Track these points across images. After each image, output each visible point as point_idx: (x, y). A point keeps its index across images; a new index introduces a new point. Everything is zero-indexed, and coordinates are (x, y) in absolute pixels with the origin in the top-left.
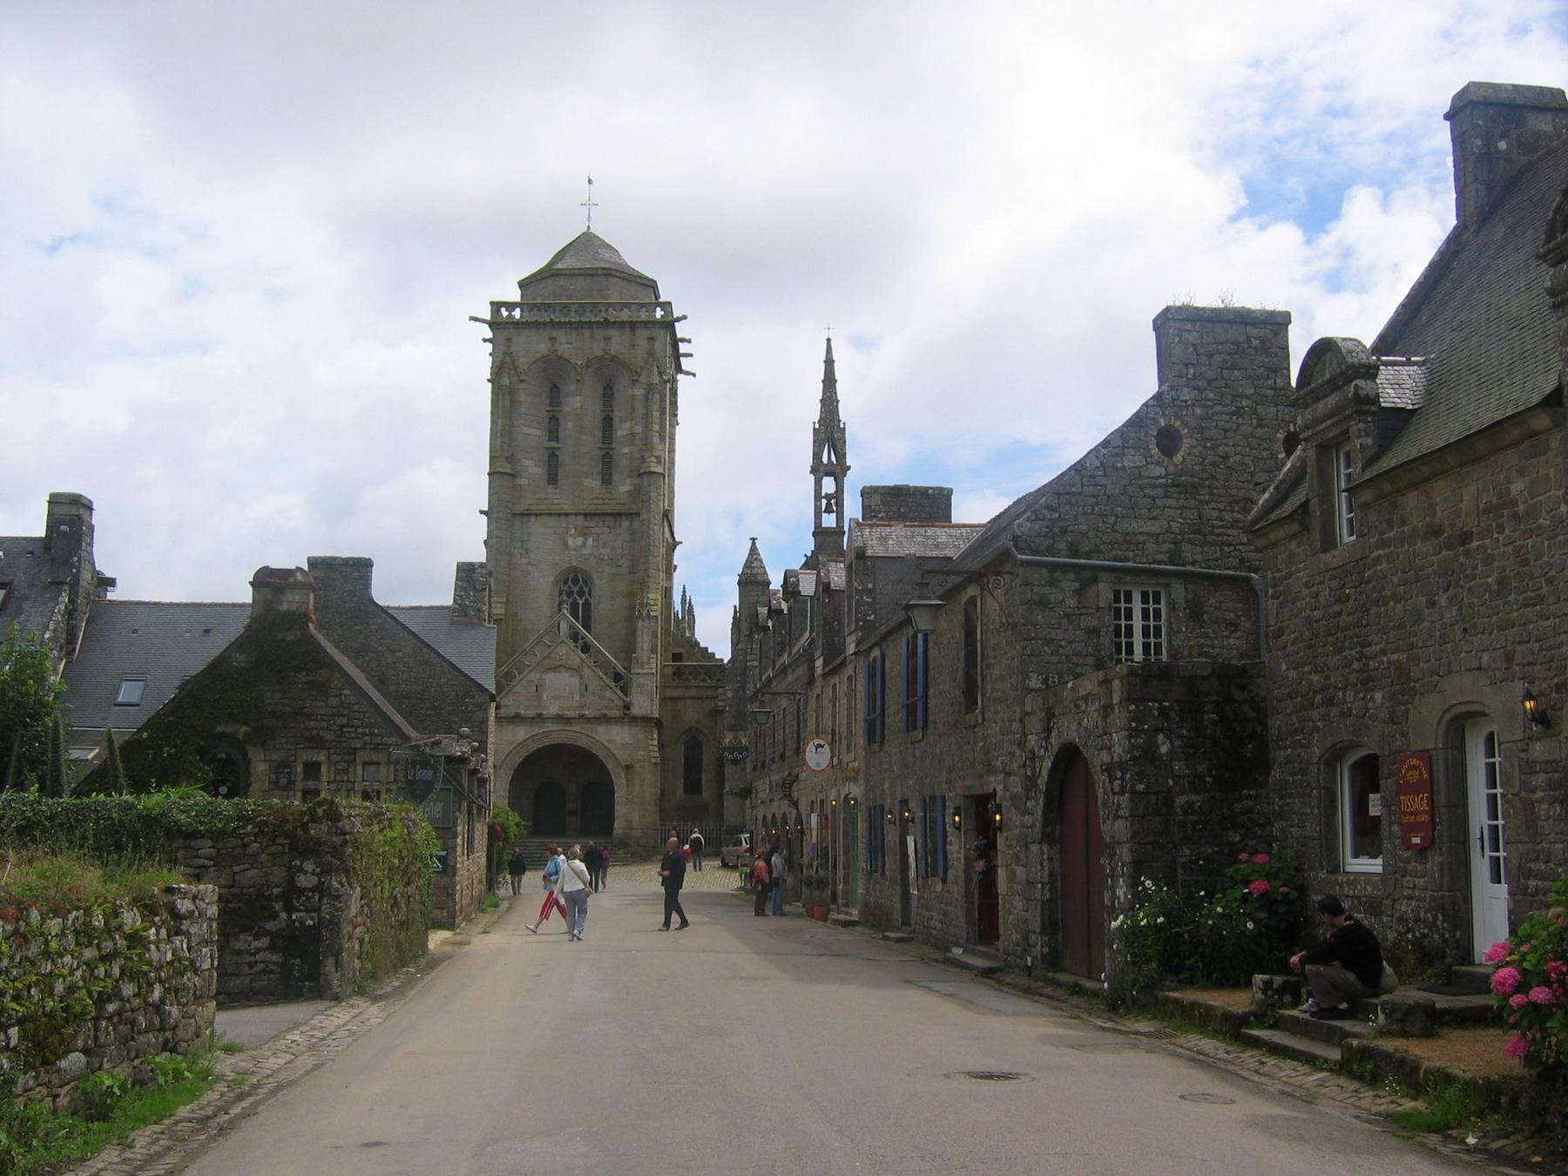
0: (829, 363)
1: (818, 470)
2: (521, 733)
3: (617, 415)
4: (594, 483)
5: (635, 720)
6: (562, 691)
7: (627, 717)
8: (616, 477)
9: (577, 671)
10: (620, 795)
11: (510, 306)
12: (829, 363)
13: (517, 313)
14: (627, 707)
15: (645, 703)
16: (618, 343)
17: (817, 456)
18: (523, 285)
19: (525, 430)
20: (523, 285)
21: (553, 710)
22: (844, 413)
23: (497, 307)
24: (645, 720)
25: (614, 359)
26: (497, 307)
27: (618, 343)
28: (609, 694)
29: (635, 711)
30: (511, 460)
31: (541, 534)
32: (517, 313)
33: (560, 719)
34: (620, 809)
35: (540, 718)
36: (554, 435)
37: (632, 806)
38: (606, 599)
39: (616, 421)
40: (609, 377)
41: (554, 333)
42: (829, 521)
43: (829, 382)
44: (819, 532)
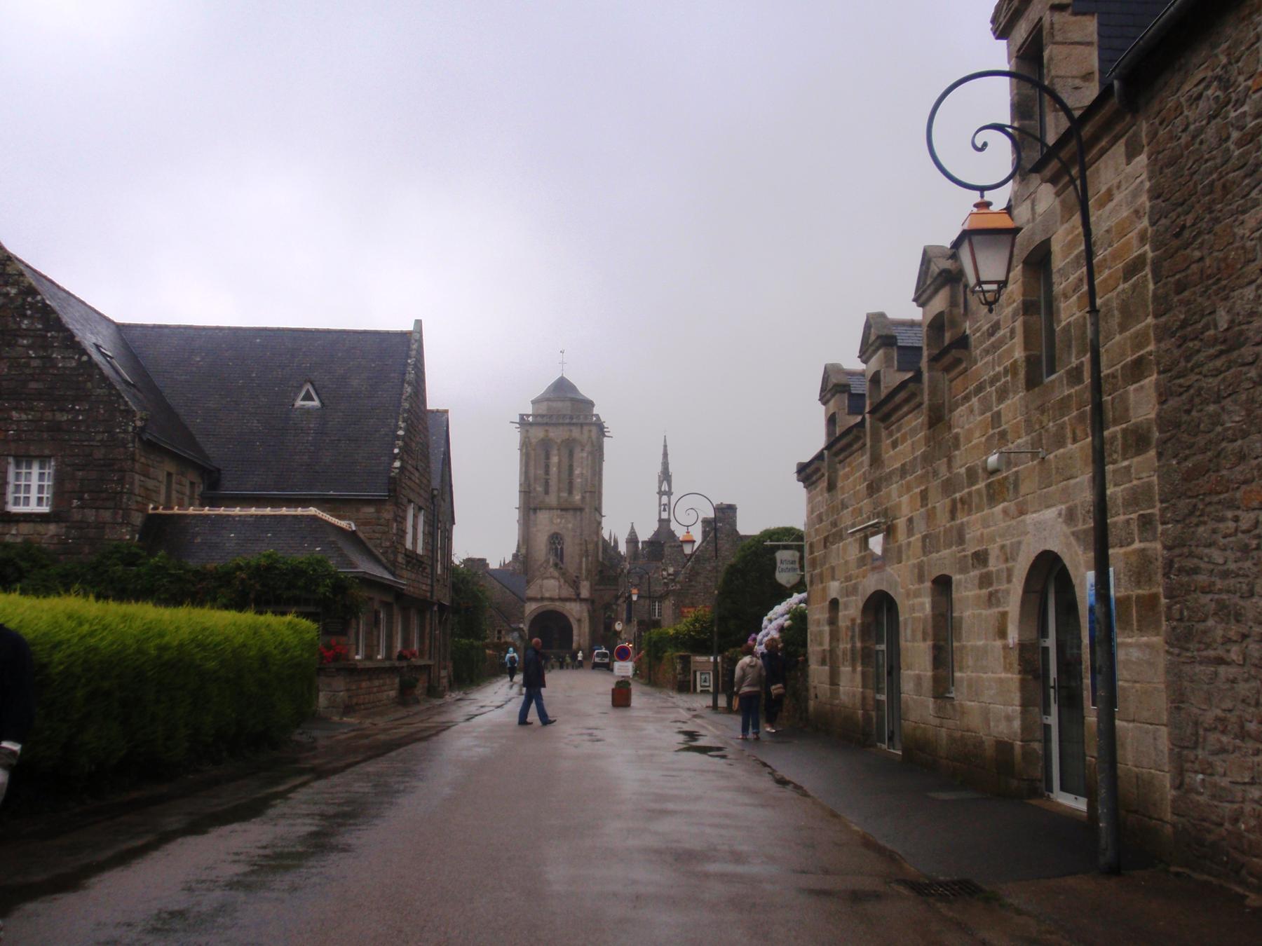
0: (665, 446)
1: (661, 493)
3: (575, 464)
4: (564, 495)
6: (550, 586)
7: (578, 598)
9: (558, 579)
10: (575, 632)
11: (528, 416)
12: (665, 446)
13: (531, 419)
15: (585, 593)
16: (576, 433)
17: (660, 488)
18: (533, 402)
20: (533, 402)
21: (547, 595)
22: (671, 470)
23: (522, 416)
25: (574, 440)
26: (522, 416)
27: (576, 433)
29: (583, 596)
30: (529, 485)
31: (543, 517)
33: (552, 599)
34: (575, 638)
35: (542, 599)
36: (547, 472)
37: (580, 634)
40: (570, 446)
42: (665, 515)
43: (665, 455)
44: (660, 520)
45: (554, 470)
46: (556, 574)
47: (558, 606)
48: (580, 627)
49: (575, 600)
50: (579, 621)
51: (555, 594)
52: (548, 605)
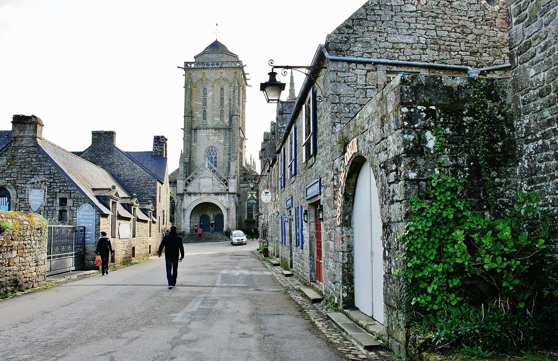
2: (193, 198)
5: (230, 193)
7: (227, 193)
8: (225, 117)
14: (227, 190)
19: (195, 102)
21: (204, 191)
24: (234, 193)
28: (222, 186)
29: (230, 191)
32: (193, 66)
34: (225, 223)
36: (205, 104)
38: (221, 157)
39: (225, 99)
41: (204, 71)
45: (209, 101)
46: (211, 174)
47: (212, 199)
48: (228, 215)
49: (224, 194)
50: (227, 210)
51: (209, 190)
52: (205, 199)
